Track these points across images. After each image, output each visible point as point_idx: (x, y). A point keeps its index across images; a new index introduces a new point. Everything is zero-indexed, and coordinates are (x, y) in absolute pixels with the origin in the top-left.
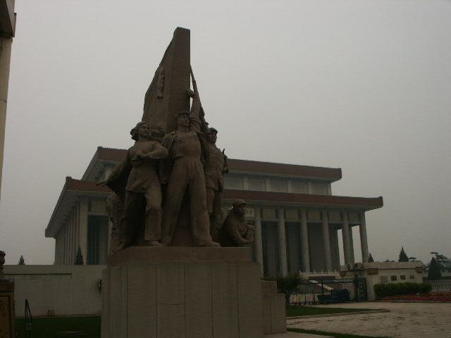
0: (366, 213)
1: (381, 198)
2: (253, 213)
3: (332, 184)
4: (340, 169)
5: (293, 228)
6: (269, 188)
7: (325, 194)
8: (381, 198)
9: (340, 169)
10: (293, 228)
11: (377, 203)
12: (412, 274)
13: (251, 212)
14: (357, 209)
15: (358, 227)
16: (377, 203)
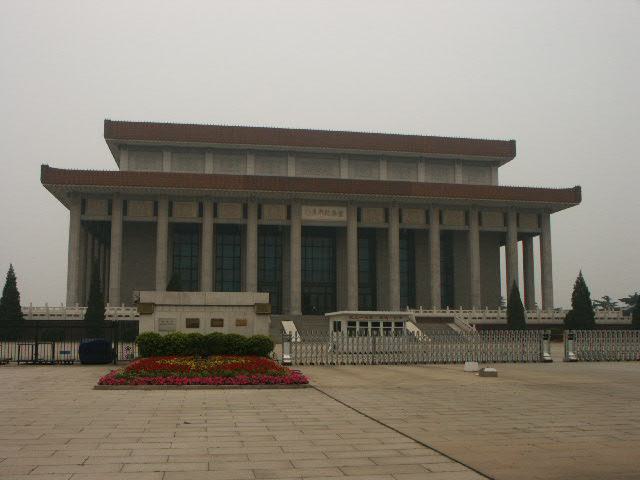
0: (553, 217)
1: (578, 190)
2: (345, 214)
3: (499, 169)
4: (512, 144)
5: (413, 240)
6: (384, 174)
7: (486, 183)
8: (578, 190)
9: (512, 144)
10: (413, 240)
11: (572, 197)
12: (241, 317)
13: (341, 214)
14: (538, 207)
15: (538, 237)
16: (572, 197)
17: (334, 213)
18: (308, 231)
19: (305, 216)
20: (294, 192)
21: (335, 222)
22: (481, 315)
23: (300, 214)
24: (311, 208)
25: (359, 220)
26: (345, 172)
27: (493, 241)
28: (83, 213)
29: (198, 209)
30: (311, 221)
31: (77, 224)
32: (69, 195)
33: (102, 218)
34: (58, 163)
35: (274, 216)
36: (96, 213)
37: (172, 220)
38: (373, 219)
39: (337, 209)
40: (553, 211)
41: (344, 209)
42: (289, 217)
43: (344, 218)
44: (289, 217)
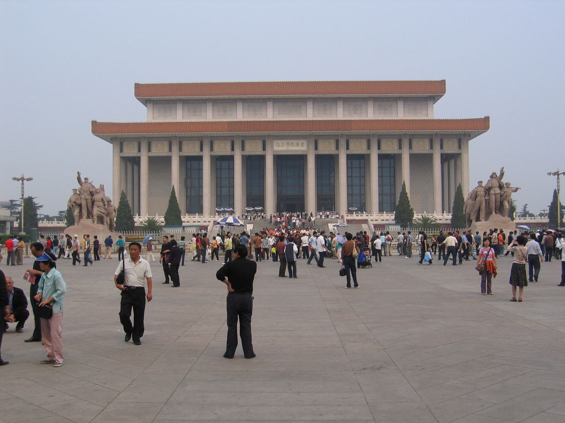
1: (487, 119)
2: (305, 145)
8: (487, 119)
11: (482, 125)
16: (482, 125)
17: (298, 145)
18: (279, 159)
19: (276, 148)
20: (267, 132)
21: (296, 151)
22: (382, 218)
23: (272, 146)
24: (280, 142)
25: (316, 148)
26: (310, 114)
27: (421, 162)
28: (121, 151)
29: (209, 144)
30: (280, 151)
31: (117, 159)
32: (112, 139)
33: (135, 155)
34: (100, 119)
35: (254, 149)
36: (130, 151)
37: (181, 154)
38: (327, 148)
39: (300, 142)
40: (470, 136)
41: (305, 142)
42: (264, 149)
43: (304, 148)
44: (264, 149)
